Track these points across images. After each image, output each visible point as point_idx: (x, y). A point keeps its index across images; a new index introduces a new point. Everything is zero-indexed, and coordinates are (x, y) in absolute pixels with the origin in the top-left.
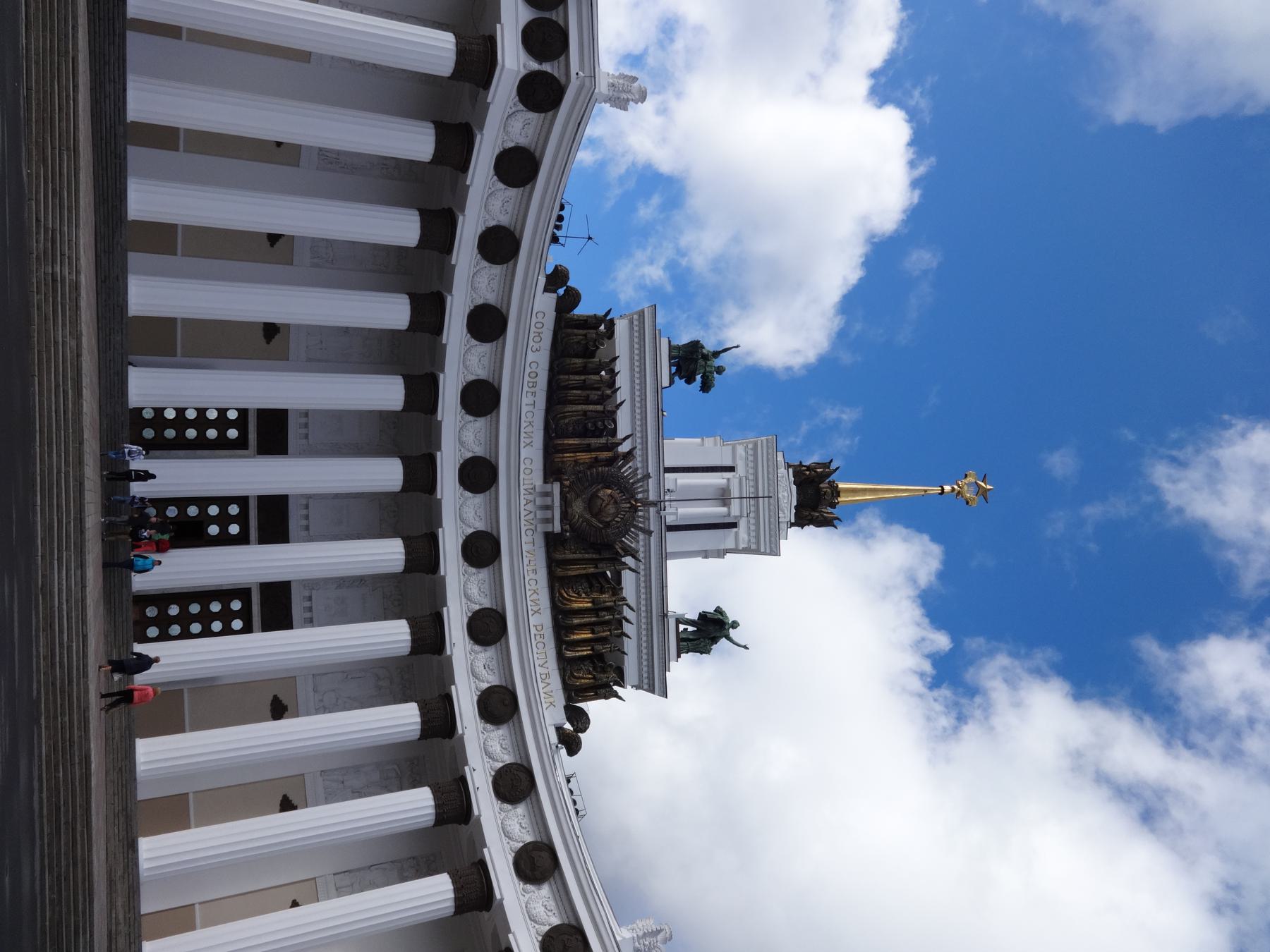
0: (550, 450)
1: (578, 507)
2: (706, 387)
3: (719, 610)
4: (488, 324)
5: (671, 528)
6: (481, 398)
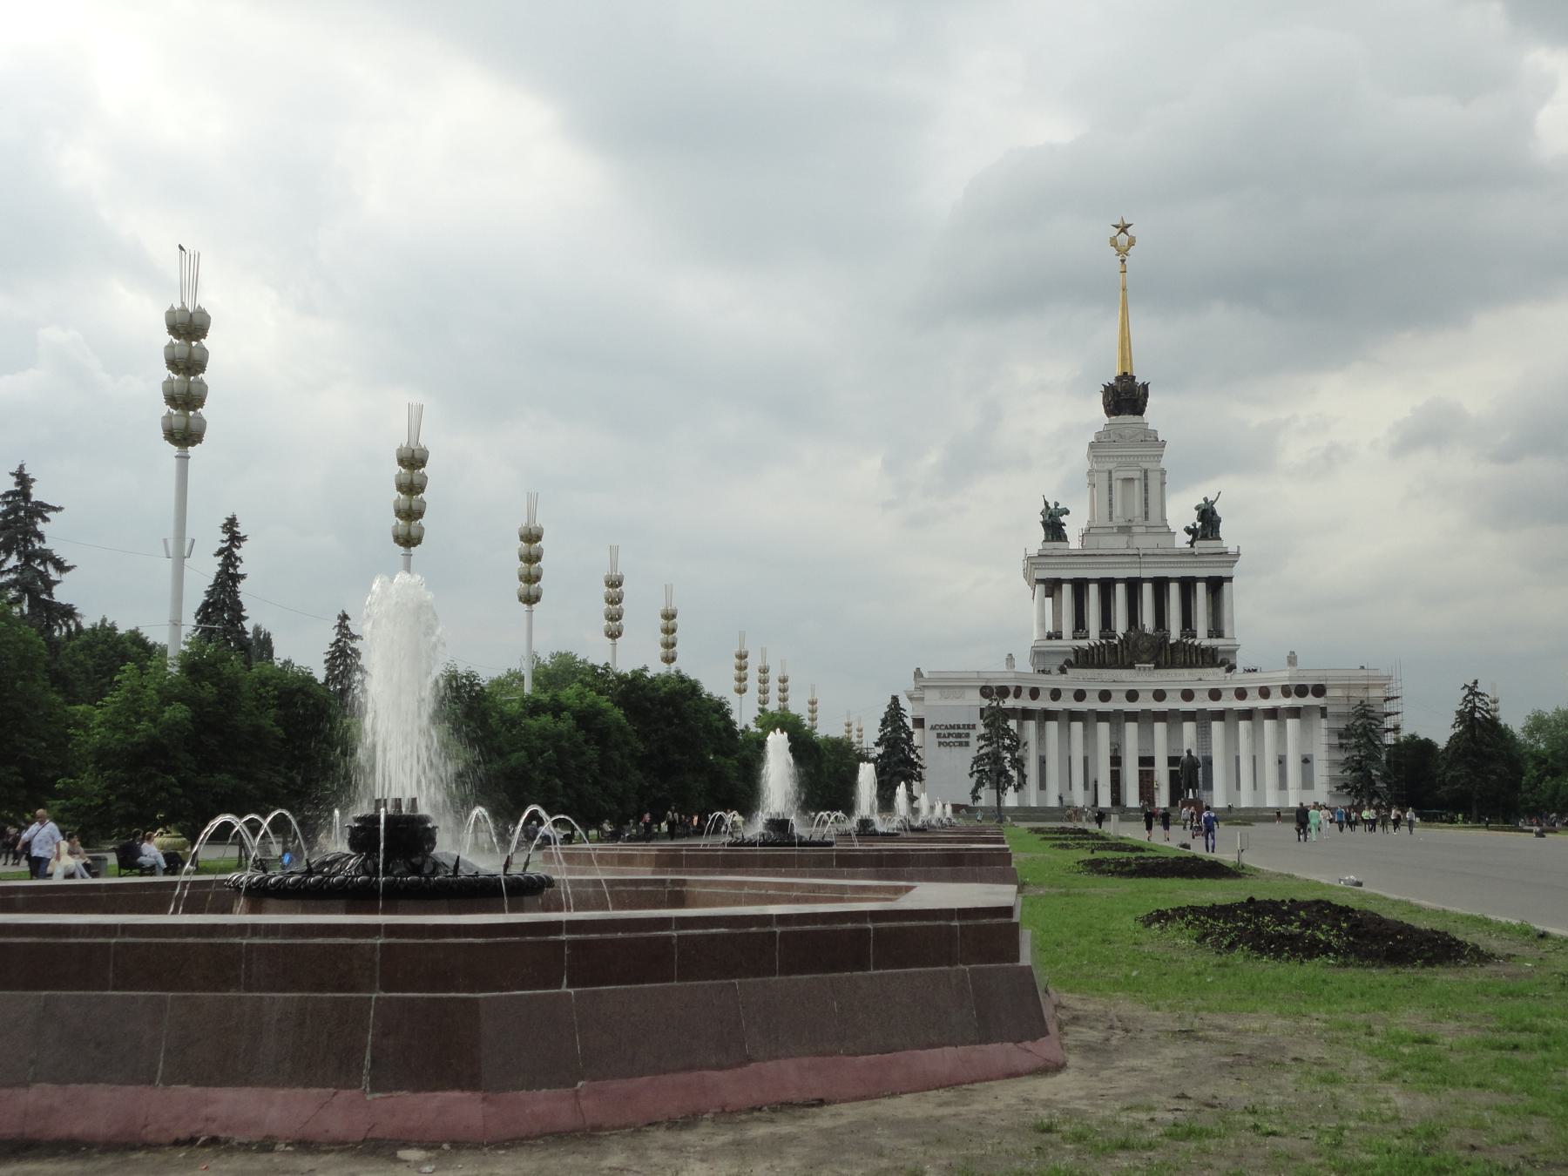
1: (1145, 657)
3: (1197, 508)
4: (1080, 695)
5: (1147, 518)
6: (1105, 696)
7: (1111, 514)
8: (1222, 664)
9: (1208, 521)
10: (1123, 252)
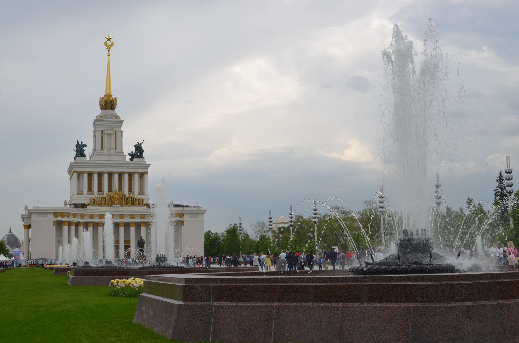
0: (108, 205)
1: (116, 202)
2: (86, 146)
3: (135, 146)
5: (116, 149)
7: (102, 147)
9: (139, 150)
10: (109, 48)
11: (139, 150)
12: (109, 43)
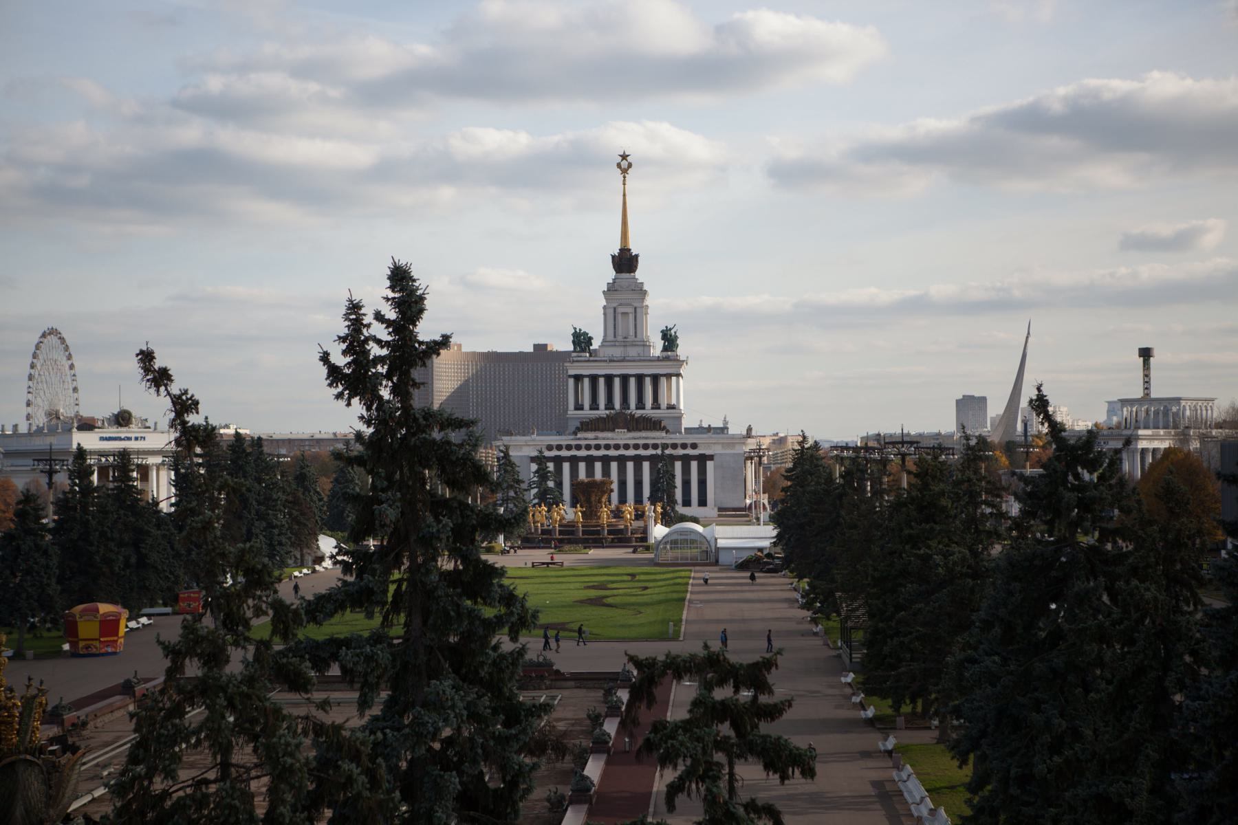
8: (664, 429)
9: (670, 340)
10: (625, 171)
11: (670, 340)
12: (624, 164)
